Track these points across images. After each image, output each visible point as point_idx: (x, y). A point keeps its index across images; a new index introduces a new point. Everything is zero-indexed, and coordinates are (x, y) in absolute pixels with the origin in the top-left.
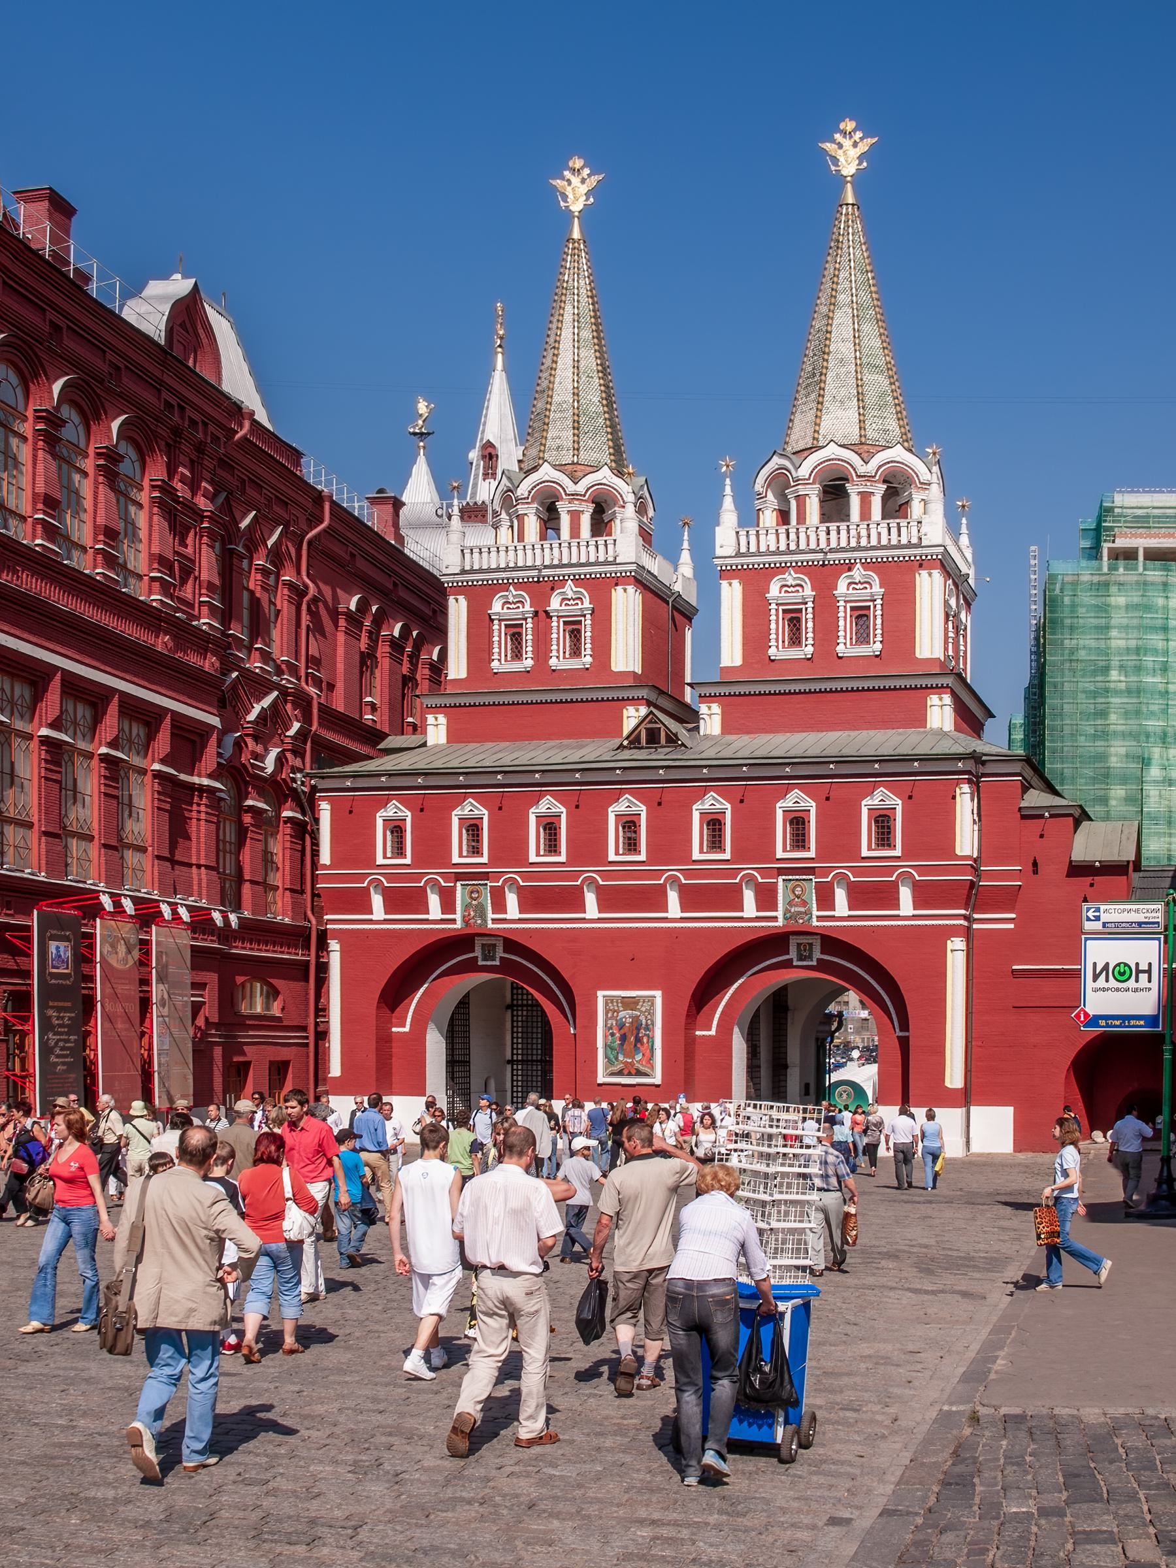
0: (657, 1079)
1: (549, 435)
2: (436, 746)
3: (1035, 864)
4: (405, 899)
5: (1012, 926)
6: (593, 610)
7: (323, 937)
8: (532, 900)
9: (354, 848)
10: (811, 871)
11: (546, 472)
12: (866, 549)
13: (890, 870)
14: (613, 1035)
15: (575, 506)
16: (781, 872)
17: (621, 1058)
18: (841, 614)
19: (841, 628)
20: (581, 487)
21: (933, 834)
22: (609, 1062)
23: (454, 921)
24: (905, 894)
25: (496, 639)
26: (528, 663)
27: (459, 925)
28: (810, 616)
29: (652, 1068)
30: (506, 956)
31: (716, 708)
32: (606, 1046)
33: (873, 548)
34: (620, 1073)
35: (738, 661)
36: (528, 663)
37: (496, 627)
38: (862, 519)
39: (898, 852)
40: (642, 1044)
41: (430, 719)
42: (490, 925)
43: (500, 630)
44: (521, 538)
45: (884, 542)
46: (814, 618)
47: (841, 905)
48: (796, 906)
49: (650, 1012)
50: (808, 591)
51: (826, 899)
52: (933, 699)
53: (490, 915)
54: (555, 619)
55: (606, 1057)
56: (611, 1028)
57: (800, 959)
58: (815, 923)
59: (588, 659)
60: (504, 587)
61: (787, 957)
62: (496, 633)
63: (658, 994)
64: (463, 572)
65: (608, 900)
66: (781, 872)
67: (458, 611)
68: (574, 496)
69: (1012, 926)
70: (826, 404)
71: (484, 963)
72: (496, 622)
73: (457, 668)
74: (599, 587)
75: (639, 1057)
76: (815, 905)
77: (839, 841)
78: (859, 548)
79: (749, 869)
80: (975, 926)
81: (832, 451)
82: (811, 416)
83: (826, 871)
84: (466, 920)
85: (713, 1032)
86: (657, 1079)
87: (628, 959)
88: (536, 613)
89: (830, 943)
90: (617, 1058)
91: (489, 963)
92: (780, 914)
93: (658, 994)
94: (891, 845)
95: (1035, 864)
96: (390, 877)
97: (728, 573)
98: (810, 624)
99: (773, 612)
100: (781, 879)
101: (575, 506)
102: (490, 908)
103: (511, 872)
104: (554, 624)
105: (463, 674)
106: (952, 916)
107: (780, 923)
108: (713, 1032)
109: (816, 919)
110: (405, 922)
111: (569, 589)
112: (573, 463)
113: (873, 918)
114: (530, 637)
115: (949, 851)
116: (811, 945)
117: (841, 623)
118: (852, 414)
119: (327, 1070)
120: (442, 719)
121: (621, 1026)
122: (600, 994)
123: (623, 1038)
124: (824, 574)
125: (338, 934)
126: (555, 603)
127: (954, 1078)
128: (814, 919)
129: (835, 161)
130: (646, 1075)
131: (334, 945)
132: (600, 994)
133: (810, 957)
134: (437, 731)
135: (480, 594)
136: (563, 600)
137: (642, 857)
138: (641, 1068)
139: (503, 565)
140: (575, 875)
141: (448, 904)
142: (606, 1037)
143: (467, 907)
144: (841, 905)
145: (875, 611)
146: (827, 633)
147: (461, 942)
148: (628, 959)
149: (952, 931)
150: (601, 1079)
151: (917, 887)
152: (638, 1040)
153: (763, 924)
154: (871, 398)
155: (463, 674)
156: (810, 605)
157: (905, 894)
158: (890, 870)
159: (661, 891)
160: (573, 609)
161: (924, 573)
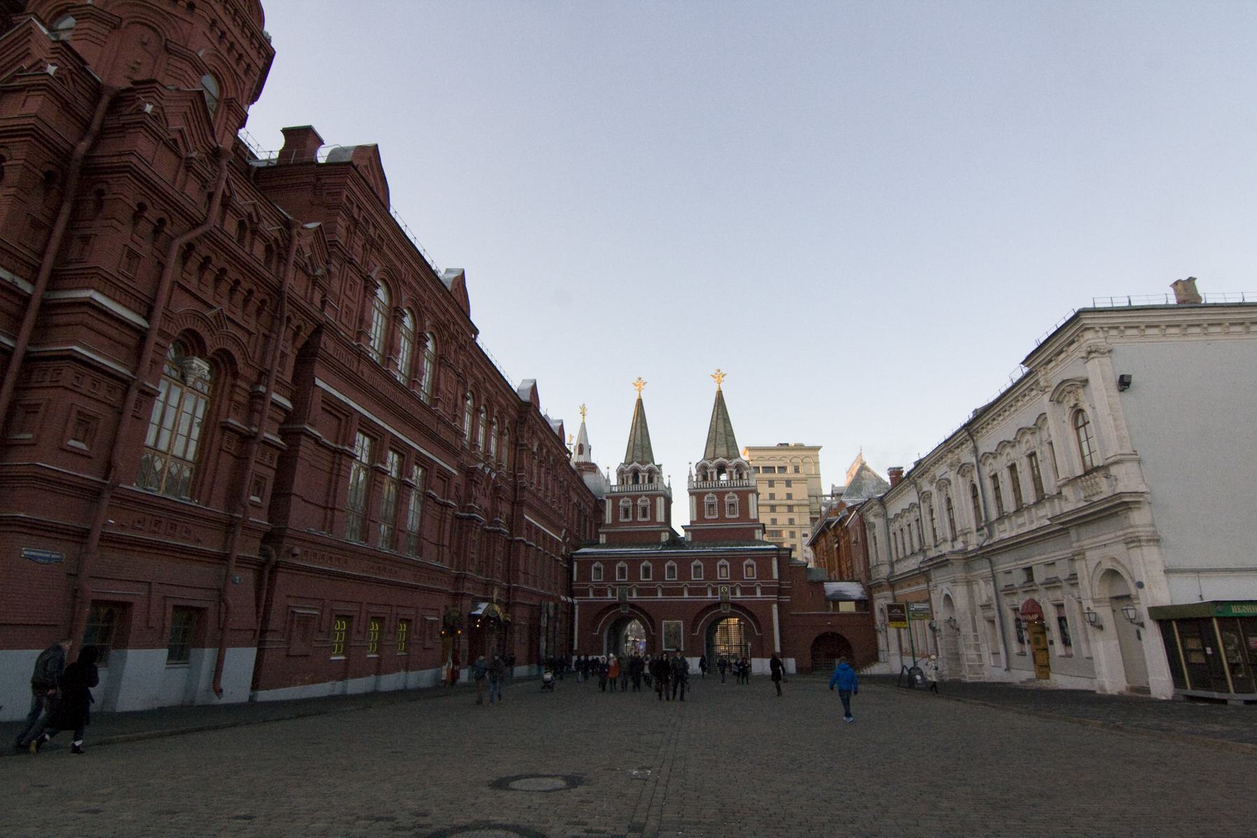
8: (640, 592)
11: (635, 464)
21: (764, 570)
24: (758, 591)
51: (734, 593)
67: (609, 504)
73: (608, 518)
74: (653, 498)
79: (709, 582)
81: (721, 459)
103: (635, 583)
110: (599, 599)
113: (748, 598)
115: (771, 578)
135: (616, 499)
141: (614, 593)
144: (739, 595)
147: (617, 605)
157: (758, 591)
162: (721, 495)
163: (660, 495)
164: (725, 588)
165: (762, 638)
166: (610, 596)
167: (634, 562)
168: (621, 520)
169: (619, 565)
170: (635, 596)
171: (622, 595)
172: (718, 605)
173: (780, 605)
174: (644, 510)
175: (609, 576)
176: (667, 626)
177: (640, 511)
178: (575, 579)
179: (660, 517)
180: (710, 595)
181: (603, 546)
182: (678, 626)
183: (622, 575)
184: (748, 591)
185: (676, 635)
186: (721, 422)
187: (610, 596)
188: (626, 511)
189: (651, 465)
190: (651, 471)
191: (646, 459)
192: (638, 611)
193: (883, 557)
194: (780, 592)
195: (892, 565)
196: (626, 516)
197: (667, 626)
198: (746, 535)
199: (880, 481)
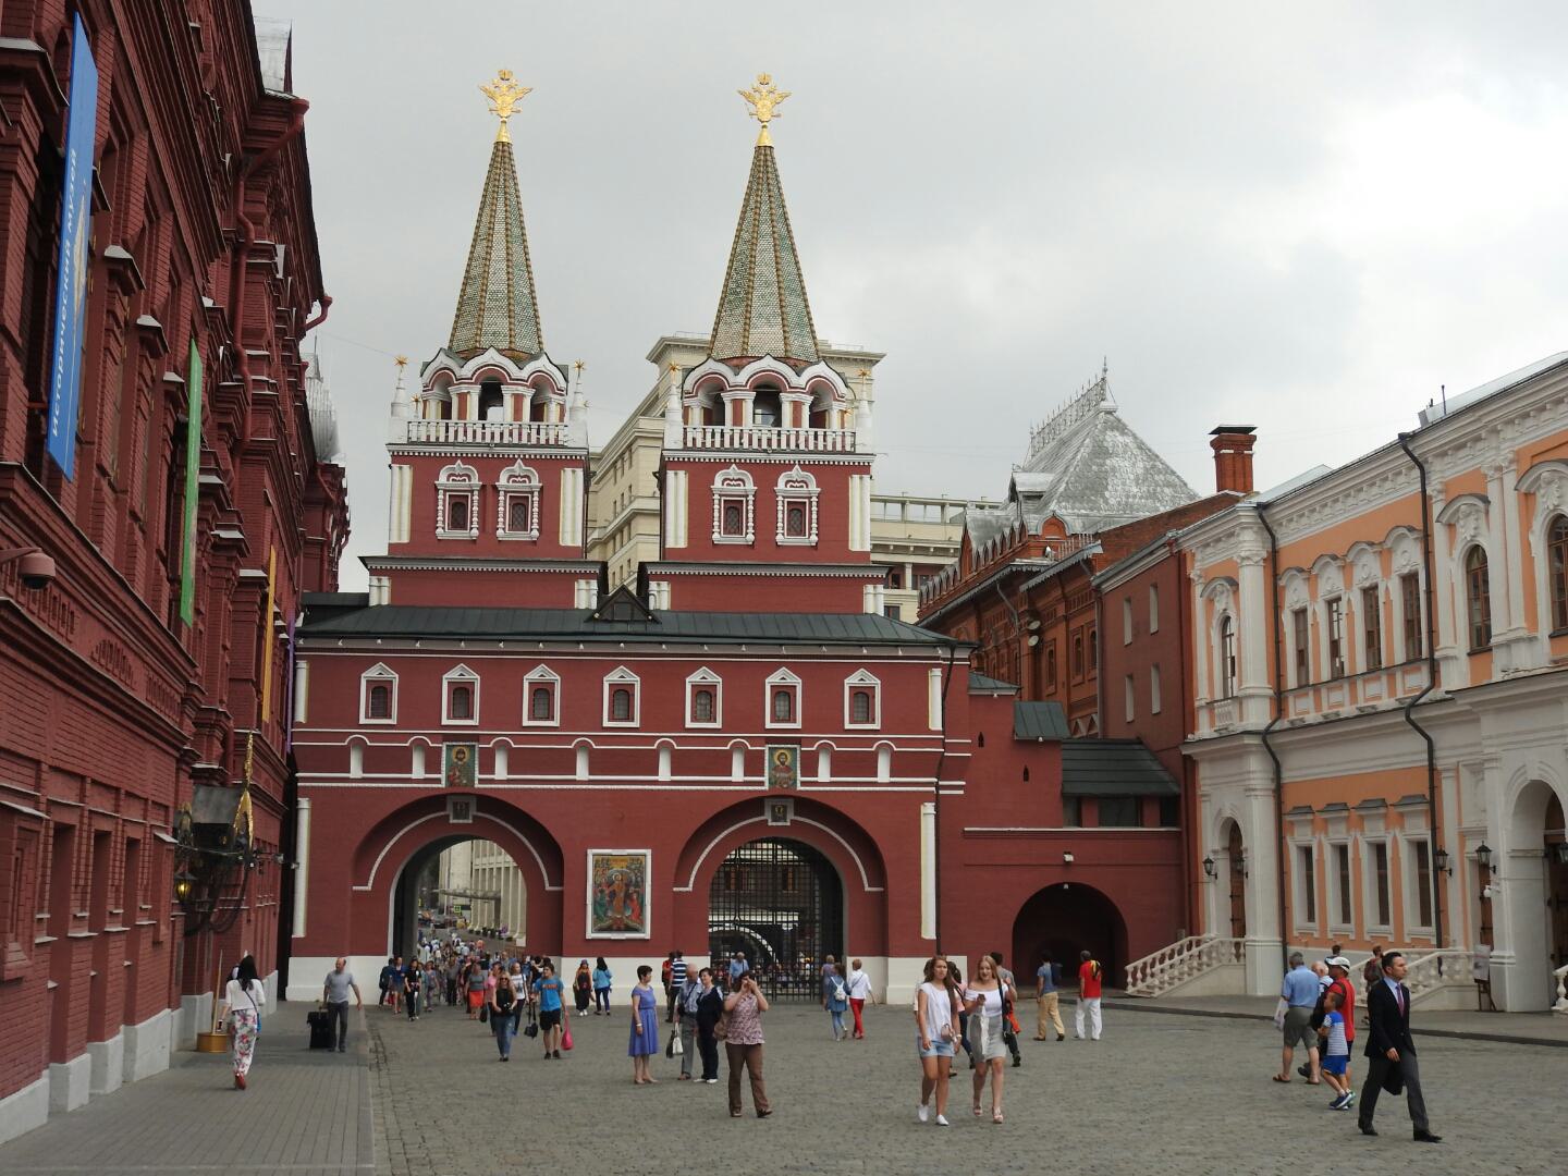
0: (647, 935)
1: (485, 321)
2: (379, 606)
3: (981, 738)
4: (385, 758)
5: (962, 792)
6: (542, 488)
7: (291, 793)
9: (333, 702)
10: (798, 741)
11: (491, 357)
12: (803, 452)
13: (871, 742)
14: (602, 891)
15: (521, 390)
16: (769, 740)
17: (610, 914)
18: (780, 508)
19: (780, 520)
20: (524, 374)
22: (597, 917)
23: (438, 781)
25: (440, 507)
27: (443, 785)
28: (751, 507)
29: (642, 923)
30: (480, 814)
31: (665, 586)
32: (595, 903)
33: (811, 452)
34: (609, 929)
35: (682, 544)
37: (441, 496)
38: (735, 424)
39: (877, 726)
40: (632, 900)
42: (477, 785)
43: (444, 501)
44: (462, 414)
45: (811, 447)
46: (754, 511)
47: (824, 773)
48: (781, 771)
49: (641, 870)
50: (750, 486)
51: (810, 767)
52: (869, 588)
53: (478, 776)
54: (502, 493)
55: (595, 912)
56: (600, 885)
57: (775, 819)
58: (799, 788)
59: (535, 533)
60: (452, 459)
61: (762, 818)
62: (441, 502)
63: (648, 852)
64: (411, 443)
65: (599, 763)
66: (769, 740)
68: (518, 381)
69: (962, 792)
70: (754, 320)
71: (456, 821)
72: (441, 492)
75: (628, 913)
76: (799, 772)
77: (823, 715)
78: (797, 451)
79: (739, 737)
80: (941, 792)
82: (738, 327)
83: (813, 741)
84: (448, 777)
85: (690, 888)
86: (647, 935)
87: (625, 819)
88: (483, 487)
89: (806, 805)
90: (605, 914)
91: (461, 821)
92: (765, 779)
93: (648, 852)
94: (870, 719)
95: (981, 738)
97: (678, 465)
98: (751, 515)
99: (716, 502)
100: (766, 748)
101: (521, 390)
102: (477, 769)
103: (503, 735)
104: (501, 498)
106: (924, 783)
108: (690, 888)
110: (387, 780)
112: (510, 349)
113: (854, 783)
114: (475, 508)
115: (922, 723)
116: (785, 807)
117: (780, 515)
118: (778, 330)
119: (291, 932)
121: (610, 884)
122: (591, 852)
123: (613, 894)
124: (765, 473)
125: (311, 793)
126: (503, 481)
127: (929, 931)
128: (799, 784)
131: (304, 803)
132: (591, 852)
136: (511, 476)
137: (636, 724)
138: (630, 923)
139: (424, 439)
141: (432, 764)
142: (595, 893)
143: (450, 767)
144: (824, 773)
145: (811, 506)
146: (765, 525)
148: (625, 819)
149: (925, 797)
150: (590, 935)
151: (895, 757)
152: (628, 896)
153: (750, 788)
154: (792, 318)
156: (751, 498)
158: (871, 742)
159: (655, 755)
161: (856, 477)
162: (765, 473)
163: (573, 462)
166: (418, 771)
168: (443, 532)
170: (501, 770)
171: (460, 770)
174: (519, 503)
176: (604, 863)
177: (503, 507)
178: (301, 716)
180: (738, 773)
182: (638, 862)
184: (855, 763)
186: (765, 244)
187: (418, 771)
189: (541, 364)
190: (540, 384)
191: (524, 343)
192: (500, 818)
193: (1255, 676)
194: (942, 767)
195: (1279, 700)
197: (604, 863)
199: (1156, 469)
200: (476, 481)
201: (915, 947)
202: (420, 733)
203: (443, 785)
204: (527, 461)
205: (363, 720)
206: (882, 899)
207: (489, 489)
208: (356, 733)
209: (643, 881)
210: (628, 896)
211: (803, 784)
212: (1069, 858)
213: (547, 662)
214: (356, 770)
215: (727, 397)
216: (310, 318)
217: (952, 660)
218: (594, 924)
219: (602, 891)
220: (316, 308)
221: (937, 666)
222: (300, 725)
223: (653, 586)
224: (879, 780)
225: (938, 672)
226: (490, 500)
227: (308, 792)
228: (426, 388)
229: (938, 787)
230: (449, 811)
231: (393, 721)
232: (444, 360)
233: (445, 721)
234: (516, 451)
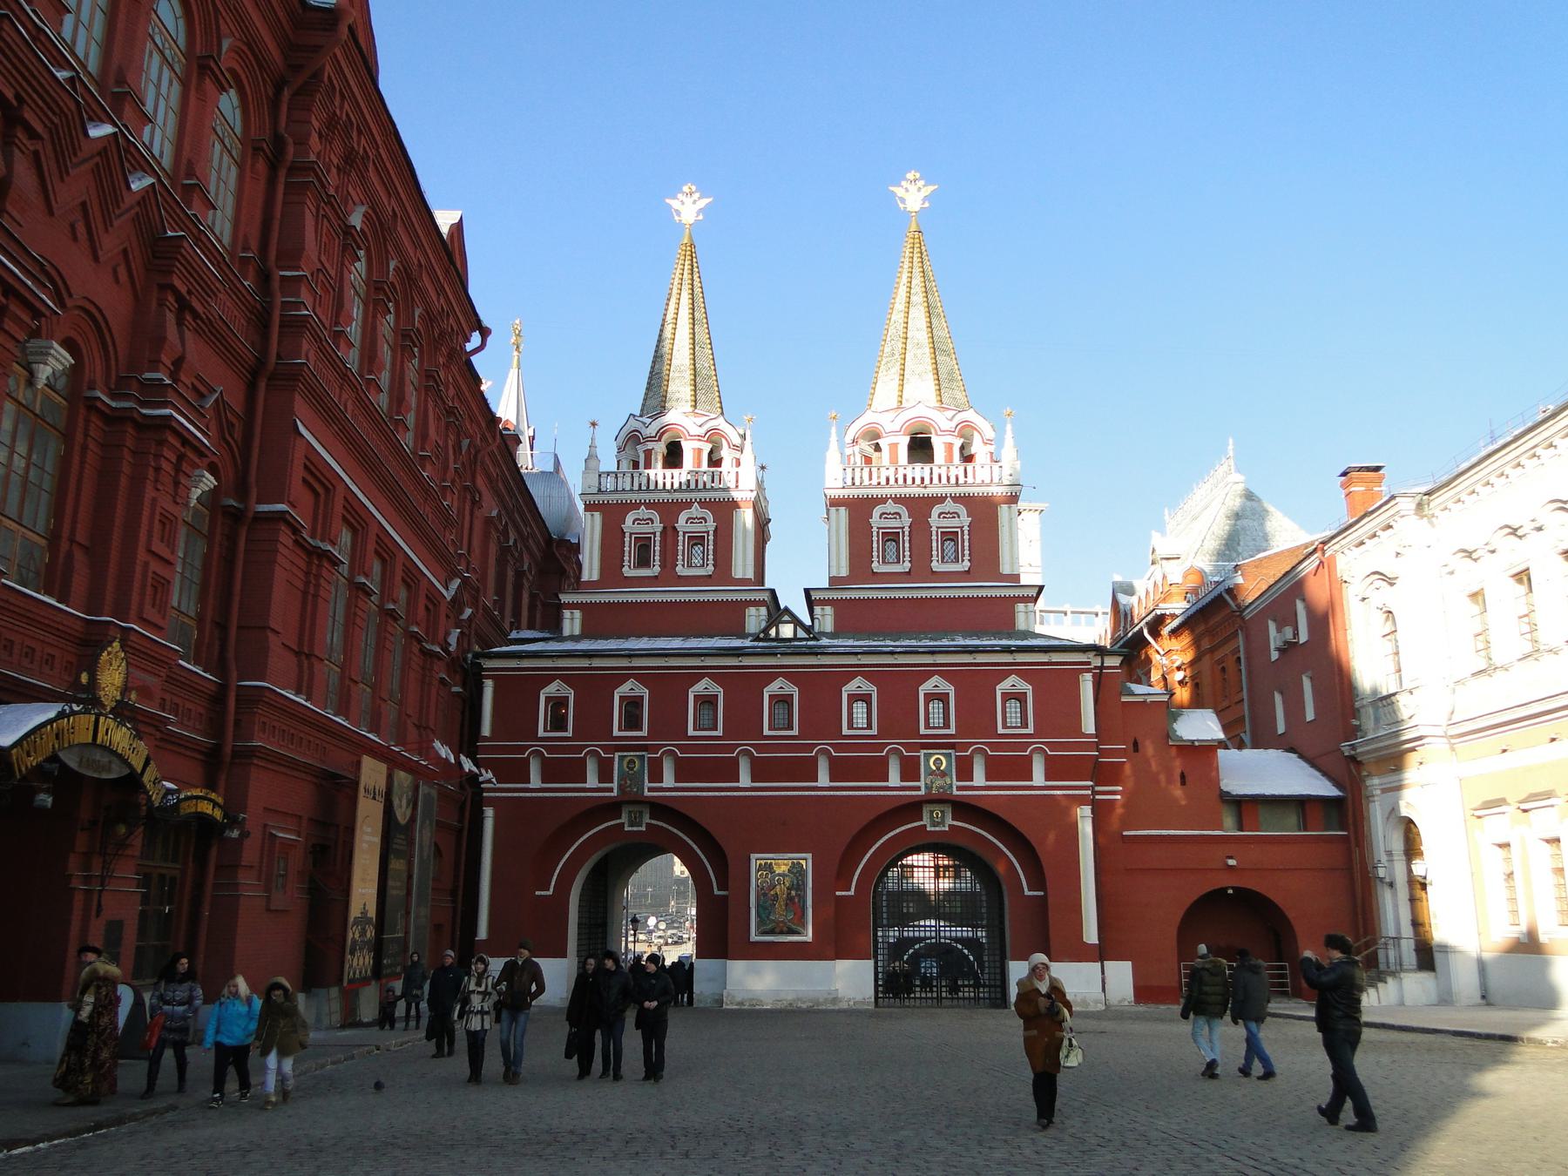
0: (808, 936)
3: (1136, 744)
8: (685, 771)
22: (761, 922)
23: (611, 790)
26: (656, 570)
27: (615, 793)
29: (804, 925)
31: (828, 610)
32: (758, 906)
34: (772, 932)
36: (656, 570)
37: (627, 539)
39: (1030, 730)
41: (567, 613)
42: (646, 793)
47: (979, 778)
50: (906, 521)
51: (965, 771)
53: (647, 784)
55: (758, 915)
58: (955, 792)
60: (636, 506)
63: (809, 856)
65: (761, 771)
73: (591, 567)
79: (894, 743)
84: (620, 786)
85: (852, 892)
89: (963, 808)
92: (922, 784)
93: (809, 856)
95: (1136, 744)
96: (550, 749)
103: (670, 744)
105: (595, 577)
107: (922, 792)
108: (852, 892)
109: (955, 787)
110: (564, 790)
111: (696, 511)
113: (1007, 789)
119: (475, 934)
120: (577, 614)
122: (753, 856)
125: (492, 802)
127: (1091, 935)
129: (903, 200)
130: (798, 933)
131: (489, 812)
133: (942, 823)
134: (572, 623)
140: (732, 748)
141: (605, 775)
143: (622, 777)
144: (979, 778)
146: (921, 554)
147: (611, 808)
150: (754, 937)
155: (595, 577)
156: (907, 530)
158: (1025, 746)
160: (697, 528)
164: (937, 760)
165: (1042, 903)
166: (592, 780)
167: (669, 686)
168: (628, 572)
169: (625, 689)
170: (669, 780)
172: (912, 808)
173: (1101, 812)
175: (594, 722)
178: (486, 730)
179: (742, 567)
180: (894, 779)
181: (572, 638)
183: (632, 721)
184: (1010, 766)
185: (794, 902)
187: (592, 780)
188: (644, 546)
196: (643, 561)
198: (998, 612)
200: (658, 526)
201: (1079, 952)
202: (593, 745)
203: (615, 793)
204: (703, 504)
205: (541, 733)
206: (1042, 903)
207: (670, 532)
208: (535, 746)
209: (804, 884)
210: (790, 898)
211: (959, 788)
212: (1232, 862)
213: (710, 676)
214: (535, 781)
215: (883, 443)
216: (469, 347)
217: (1102, 667)
218: (758, 926)
219: (765, 895)
220: (476, 339)
221: (1088, 671)
222: (486, 739)
223: (817, 610)
224: (1034, 783)
225: (1089, 676)
226: (669, 540)
227: (492, 802)
228: (620, 450)
229: (1095, 793)
230: (624, 819)
231: (569, 734)
232: (634, 424)
233: (616, 733)
234: (693, 495)
